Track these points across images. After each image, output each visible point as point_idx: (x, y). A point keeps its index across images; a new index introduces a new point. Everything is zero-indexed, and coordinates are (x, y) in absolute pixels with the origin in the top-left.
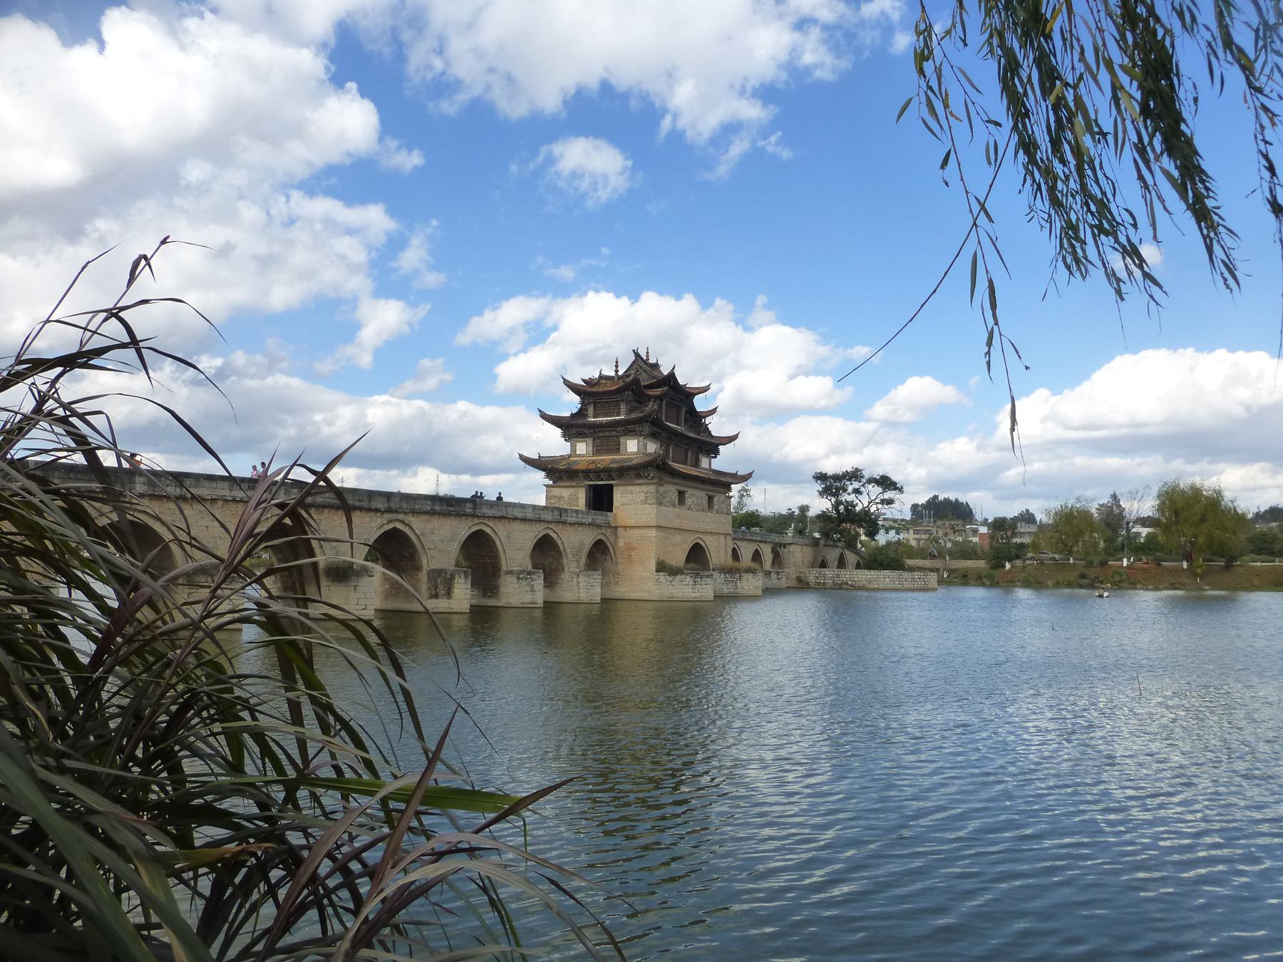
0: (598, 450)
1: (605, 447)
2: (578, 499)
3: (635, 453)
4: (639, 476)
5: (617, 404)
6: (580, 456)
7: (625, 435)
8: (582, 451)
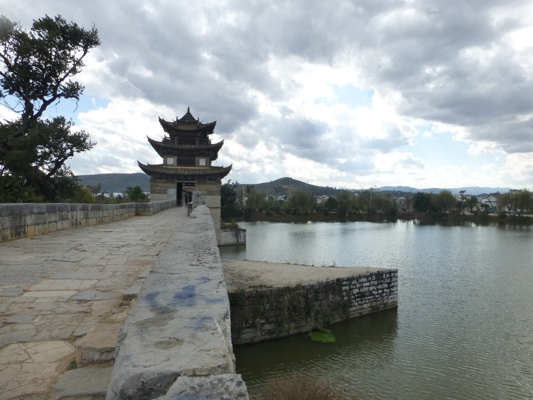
0: (179, 163)
4: (210, 179)
7: (199, 156)
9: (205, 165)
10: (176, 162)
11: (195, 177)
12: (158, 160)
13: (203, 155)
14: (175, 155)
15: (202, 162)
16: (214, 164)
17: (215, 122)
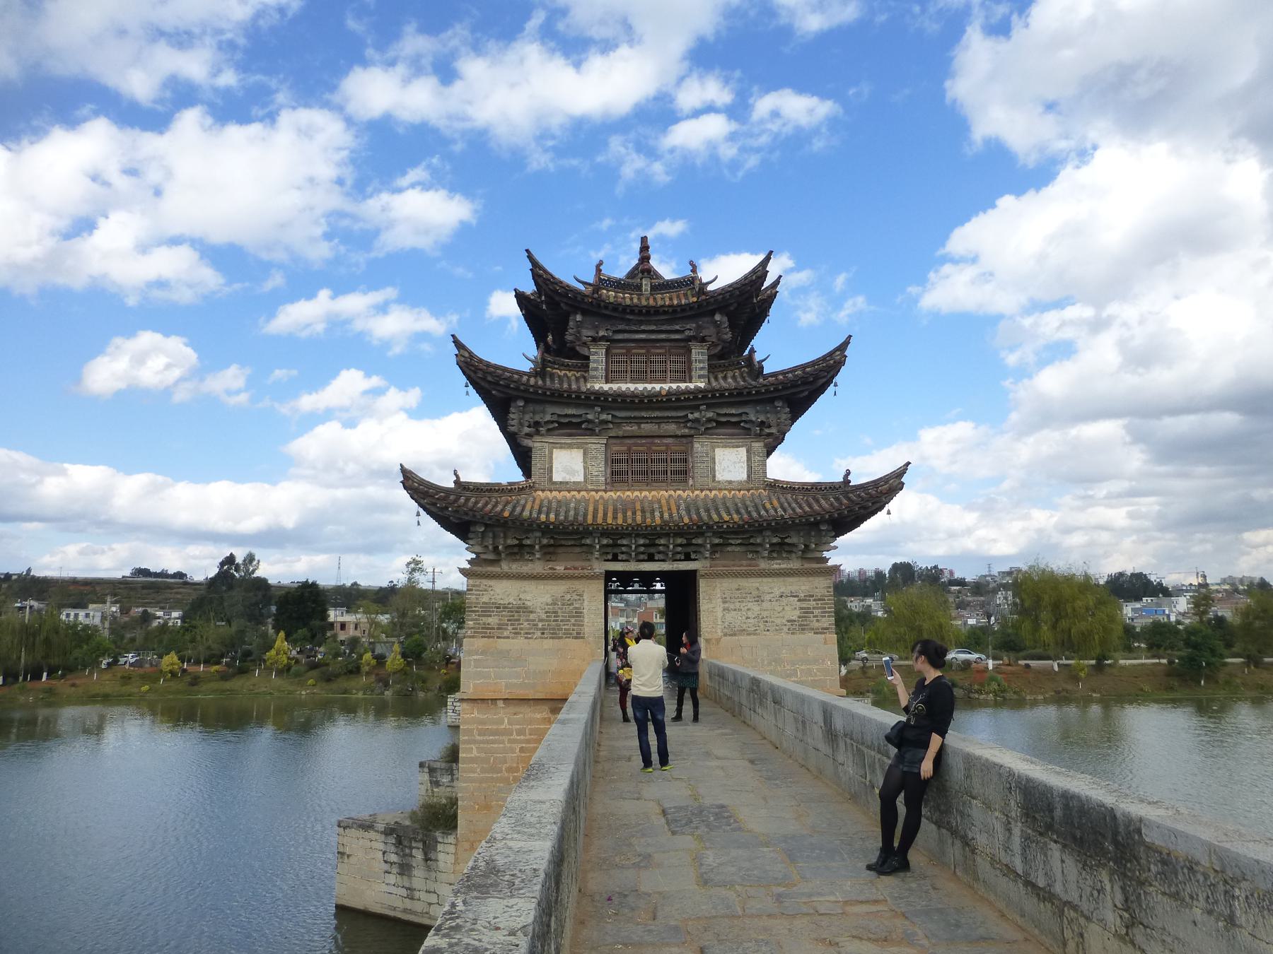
0: (617, 477)
1: (637, 467)
2: (579, 614)
3: (740, 486)
4: (781, 549)
5: (684, 347)
6: (564, 486)
8: (573, 472)
9: (744, 476)
10: (600, 469)
11: (700, 541)
13: (736, 429)
14: (591, 432)
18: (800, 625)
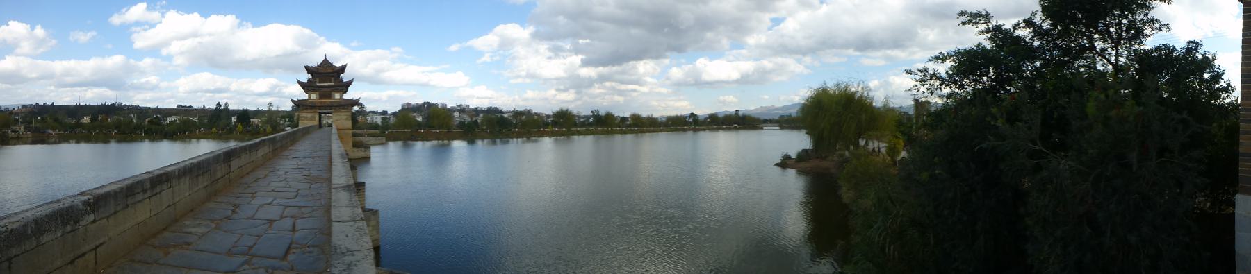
0: (321, 97)
4: (344, 108)
10: (318, 96)
12: (305, 96)
13: (338, 91)
15: (337, 96)
16: (346, 96)
17: (346, 66)
18: (346, 119)
